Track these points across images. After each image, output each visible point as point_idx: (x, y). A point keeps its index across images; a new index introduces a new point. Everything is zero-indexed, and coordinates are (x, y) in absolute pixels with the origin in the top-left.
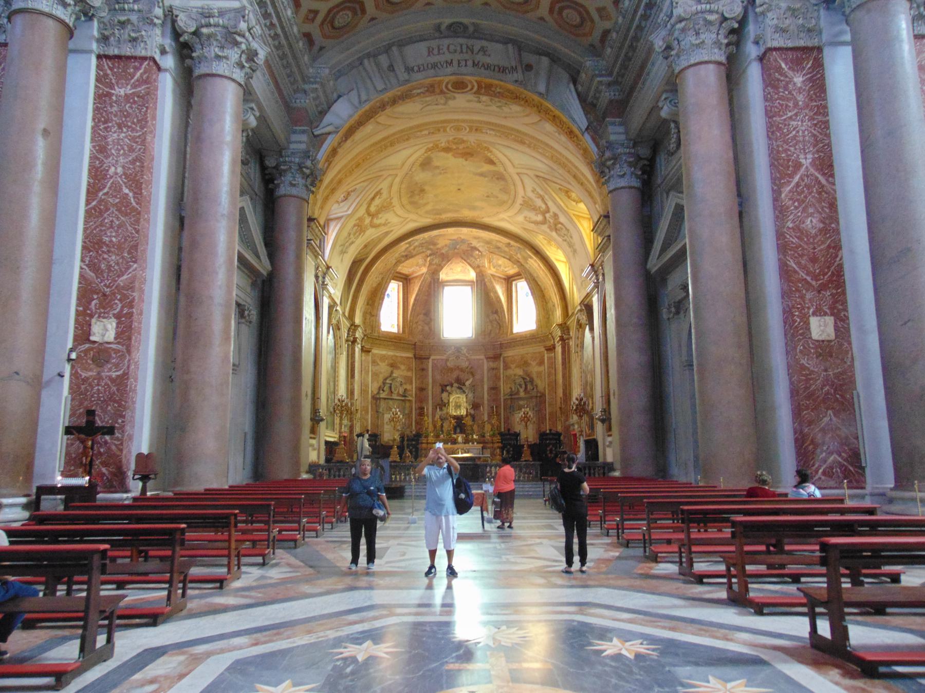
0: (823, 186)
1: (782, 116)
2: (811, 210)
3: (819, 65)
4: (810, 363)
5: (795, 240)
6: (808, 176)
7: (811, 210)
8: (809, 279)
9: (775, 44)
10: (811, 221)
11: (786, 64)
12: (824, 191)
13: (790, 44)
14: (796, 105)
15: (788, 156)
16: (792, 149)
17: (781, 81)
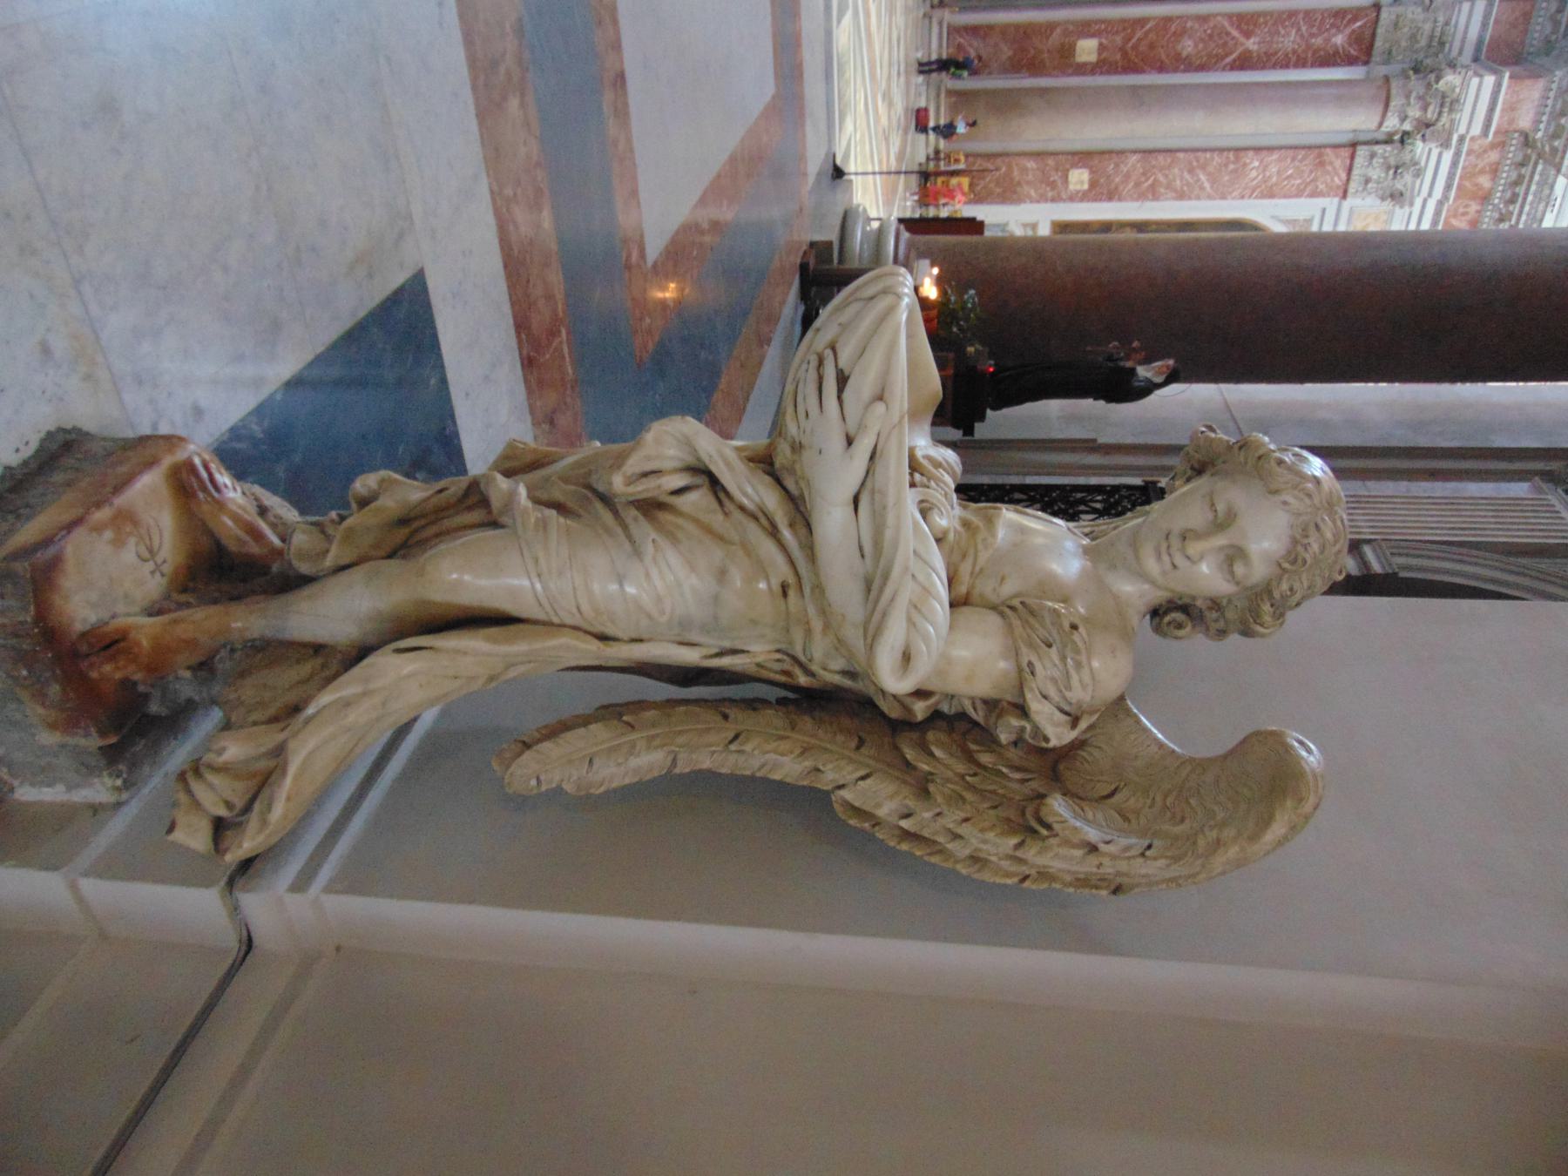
0: (1223, 58)
1: (1304, 19)
2: (1201, 46)
3: (1351, 61)
4: (1056, 38)
5: (1173, 29)
6: (1236, 44)
7: (1201, 46)
8: (1134, 40)
9: (1384, 15)
10: (1189, 46)
11: (1360, 27)
12: (1217, 60)
13: (1380, 31)
14: (1312, 35)
15: (1260, 25)
16: (1266, 30)
17: (1342, 22)
